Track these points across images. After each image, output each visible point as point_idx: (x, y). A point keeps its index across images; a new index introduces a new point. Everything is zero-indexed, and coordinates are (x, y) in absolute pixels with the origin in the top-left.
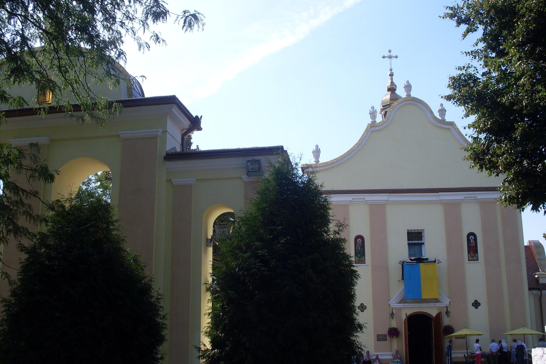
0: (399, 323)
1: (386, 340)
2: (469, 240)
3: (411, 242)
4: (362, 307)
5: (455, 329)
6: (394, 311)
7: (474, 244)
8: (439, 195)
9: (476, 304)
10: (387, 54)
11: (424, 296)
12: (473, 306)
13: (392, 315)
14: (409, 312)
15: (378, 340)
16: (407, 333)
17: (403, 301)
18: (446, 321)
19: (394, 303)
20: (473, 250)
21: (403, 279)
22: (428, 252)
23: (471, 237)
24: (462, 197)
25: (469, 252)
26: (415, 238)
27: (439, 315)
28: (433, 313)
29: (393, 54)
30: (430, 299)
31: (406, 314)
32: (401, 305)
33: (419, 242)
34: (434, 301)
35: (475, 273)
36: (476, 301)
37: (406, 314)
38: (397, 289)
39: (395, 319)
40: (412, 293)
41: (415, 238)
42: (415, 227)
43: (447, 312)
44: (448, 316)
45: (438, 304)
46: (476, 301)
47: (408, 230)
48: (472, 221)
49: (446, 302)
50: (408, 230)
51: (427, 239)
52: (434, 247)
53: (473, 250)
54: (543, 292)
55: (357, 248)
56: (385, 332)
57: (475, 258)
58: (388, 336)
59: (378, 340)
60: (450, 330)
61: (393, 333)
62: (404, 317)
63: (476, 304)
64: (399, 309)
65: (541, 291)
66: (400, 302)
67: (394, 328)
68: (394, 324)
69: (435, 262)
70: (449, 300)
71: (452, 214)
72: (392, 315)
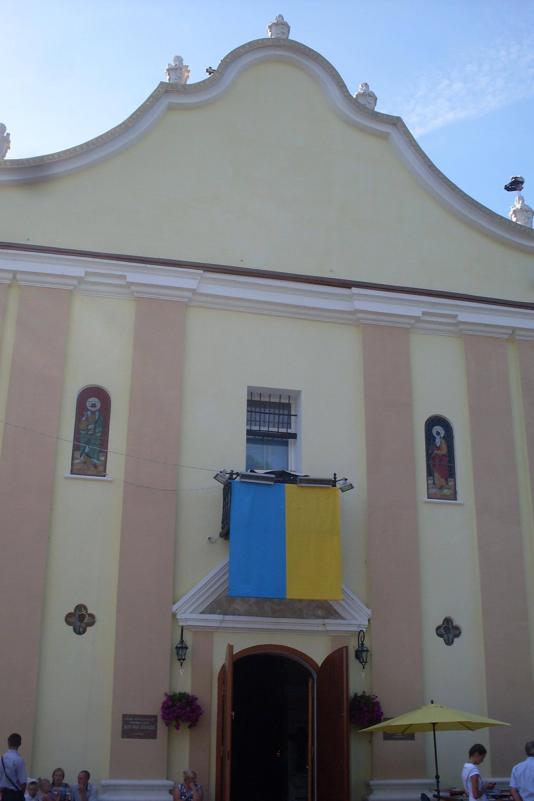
0: (203, 680)
1: (153, 735)
2: (430, 438)
3: (255, 428)
4: (81, 618)
5: (386, 707)
6: (188, 639)
7: (444, 451)
8: (351, 297)
9: (449, 631)
11: (295, 591)
12: (440, 635)
13: (181, 649)
14: (242, 644)
15: (127, 733)
16: (230, 714)
17: (221, 606)
18: (358, 681)
19: (189, 612)
20: (441, 465)
21: (225, 534)
22: (308, 457)
23: (437, 429)
24: (416, 312)
25: (430, 473)
26: (271, 417)
27: (336, 663)
28: (318, 652)
30: (311, 601)
31: (231, 648)
32: (214, 620)
33: (284, 430)
34: (320, 612)
36: (448, 621)
37: (231, 648)
38: (203, 568)
39: (188, 663)
40: (253, 587)
41: (271, 417)
42: (275, 379)
43: (361, 654)
44: (363, 662)
45: (333, 625)
46: (448, 621)
47: (251, 392)
48: (440, 384)
49: (357, 617)
50: (251, 392)
51: (309, 423)
52: (329, 441)
53: (441, 465)
55: (82, 426)
56: (152, 706)
57: (446, 491)
58: (161, 723)
59: (127, 733)
60: (367, 711)
61: (181, 710)
62: (220, 660)
63: (449, 631)
64: (207, 633)
66: (211, 609)
67: (183, 696)
68: (184, 683)
69: (333, 483)
70: (369, 611)
71: (385, 355)
72: (181, 649)
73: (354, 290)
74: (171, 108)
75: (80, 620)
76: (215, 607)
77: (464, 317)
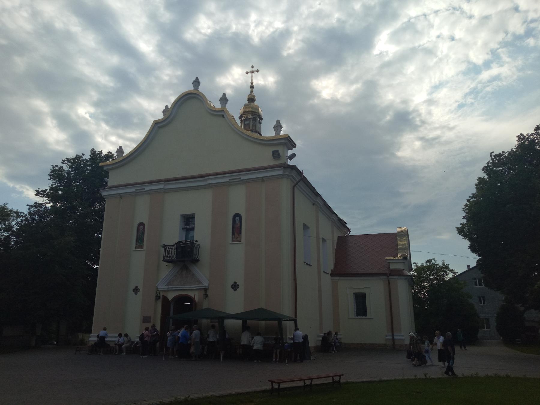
7: (239, 225)
8: (206, 180)
10: (250, 70)
12: (232, 288)
19: (162, 286)
20: (237, 230)
23: (238, 218)
24: (227, 180)
29: (254, 69)
35: (237, 253)
36: (235, 283)
42: (188, 211)
46: (235, 283)
49: (206, 284)
53: (237, 230)
54: (391, 277)
57: (238, 239)
63: (235, 286)
65: (388, 277)
73: (206, 178)
74: (160, 127)
75: (136, 290)
76: (169, 284)
77: (243, 178)
